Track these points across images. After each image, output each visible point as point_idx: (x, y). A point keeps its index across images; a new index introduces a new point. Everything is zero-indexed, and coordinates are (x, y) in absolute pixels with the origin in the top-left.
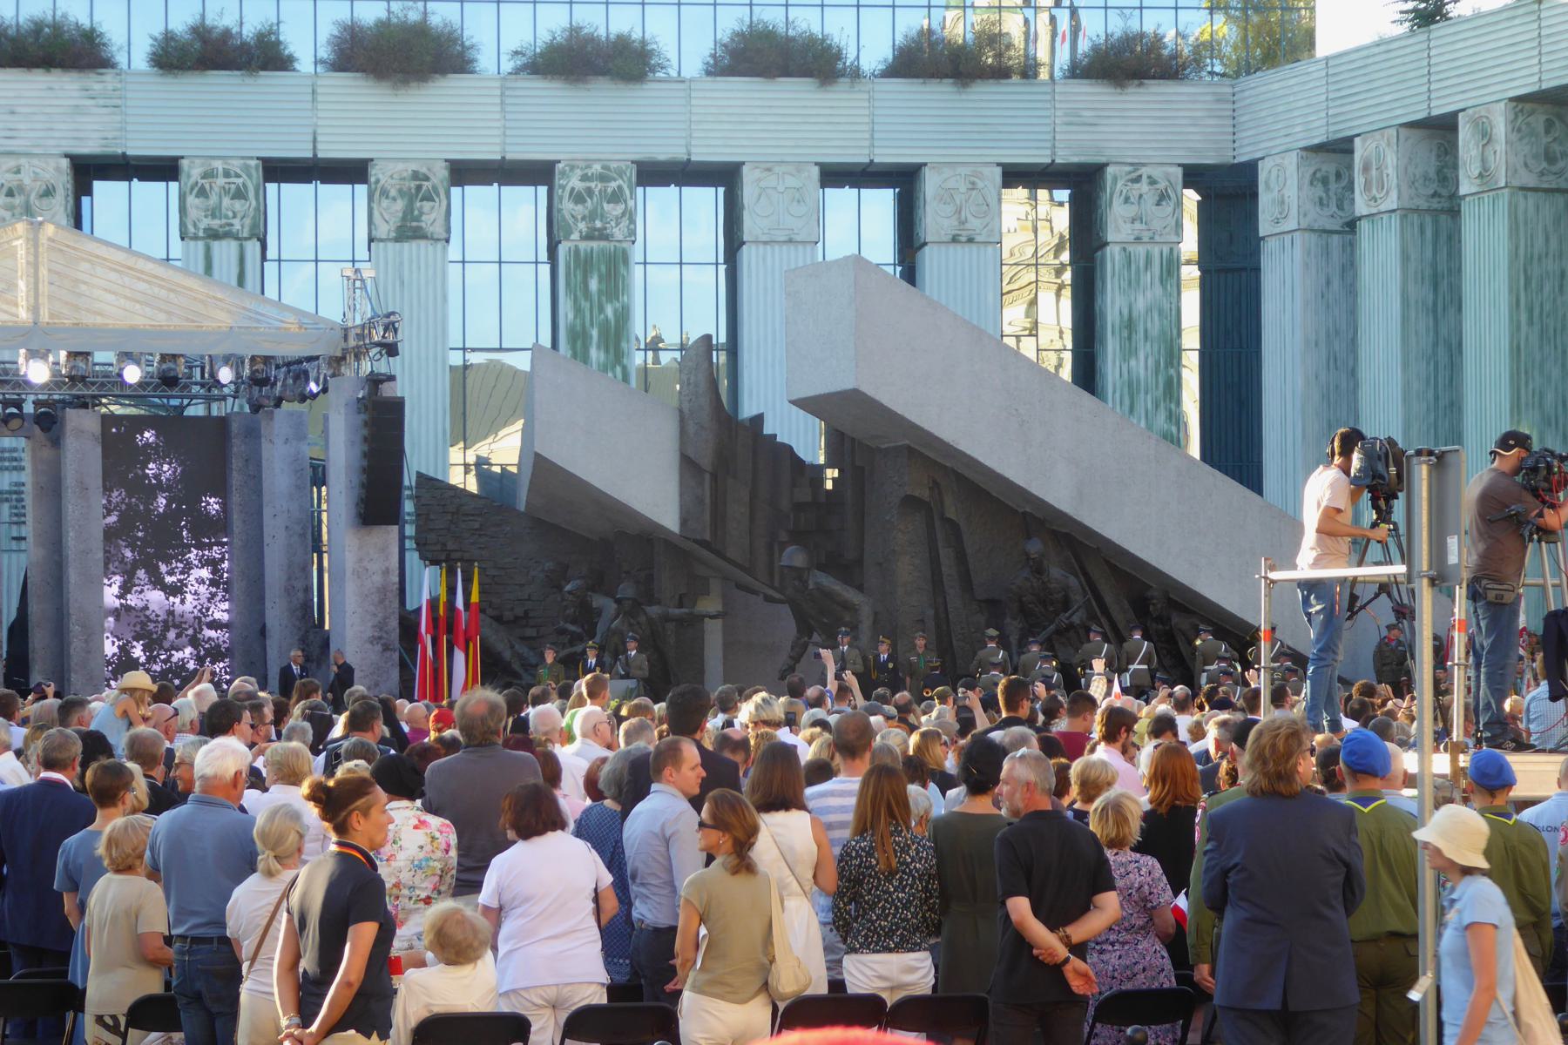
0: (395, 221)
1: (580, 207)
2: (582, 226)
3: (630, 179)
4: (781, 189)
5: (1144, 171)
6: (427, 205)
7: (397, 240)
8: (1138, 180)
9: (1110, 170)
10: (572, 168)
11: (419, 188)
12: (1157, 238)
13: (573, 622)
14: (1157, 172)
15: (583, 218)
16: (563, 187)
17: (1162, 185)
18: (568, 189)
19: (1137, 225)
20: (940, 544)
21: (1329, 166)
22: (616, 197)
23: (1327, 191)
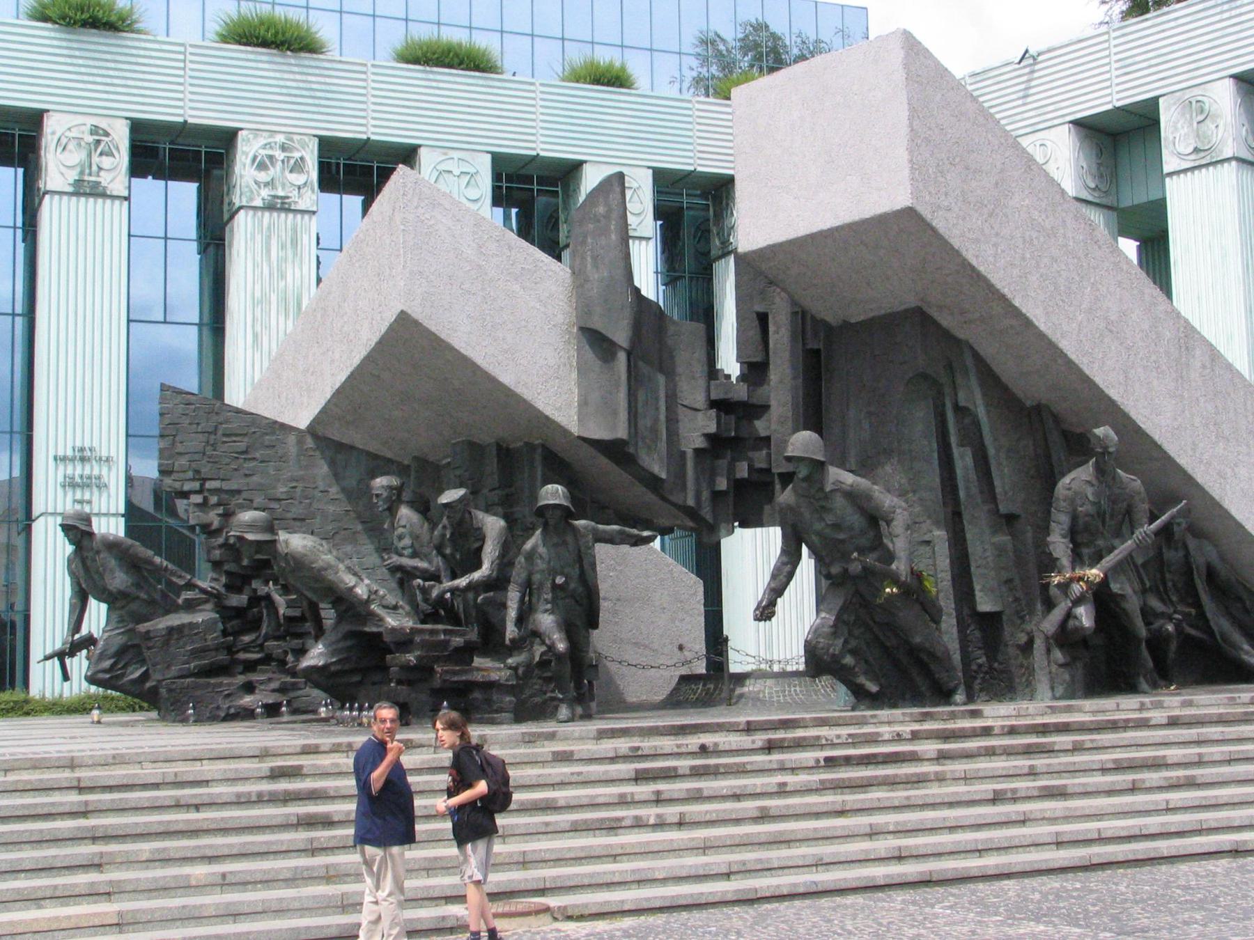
0: (73, 176)
1: (263, 176)
2: (265, 193)
3: (312, 151)
4: (457, 172)
6: (106, 162)
7: (76, 194)
10: (256, 136)
11: (98, 142)
13: (415, 555)
15: (266, 184)
16: (246, 154)
18: (251, 156)
20: (953, 440)
22: (298, 167)
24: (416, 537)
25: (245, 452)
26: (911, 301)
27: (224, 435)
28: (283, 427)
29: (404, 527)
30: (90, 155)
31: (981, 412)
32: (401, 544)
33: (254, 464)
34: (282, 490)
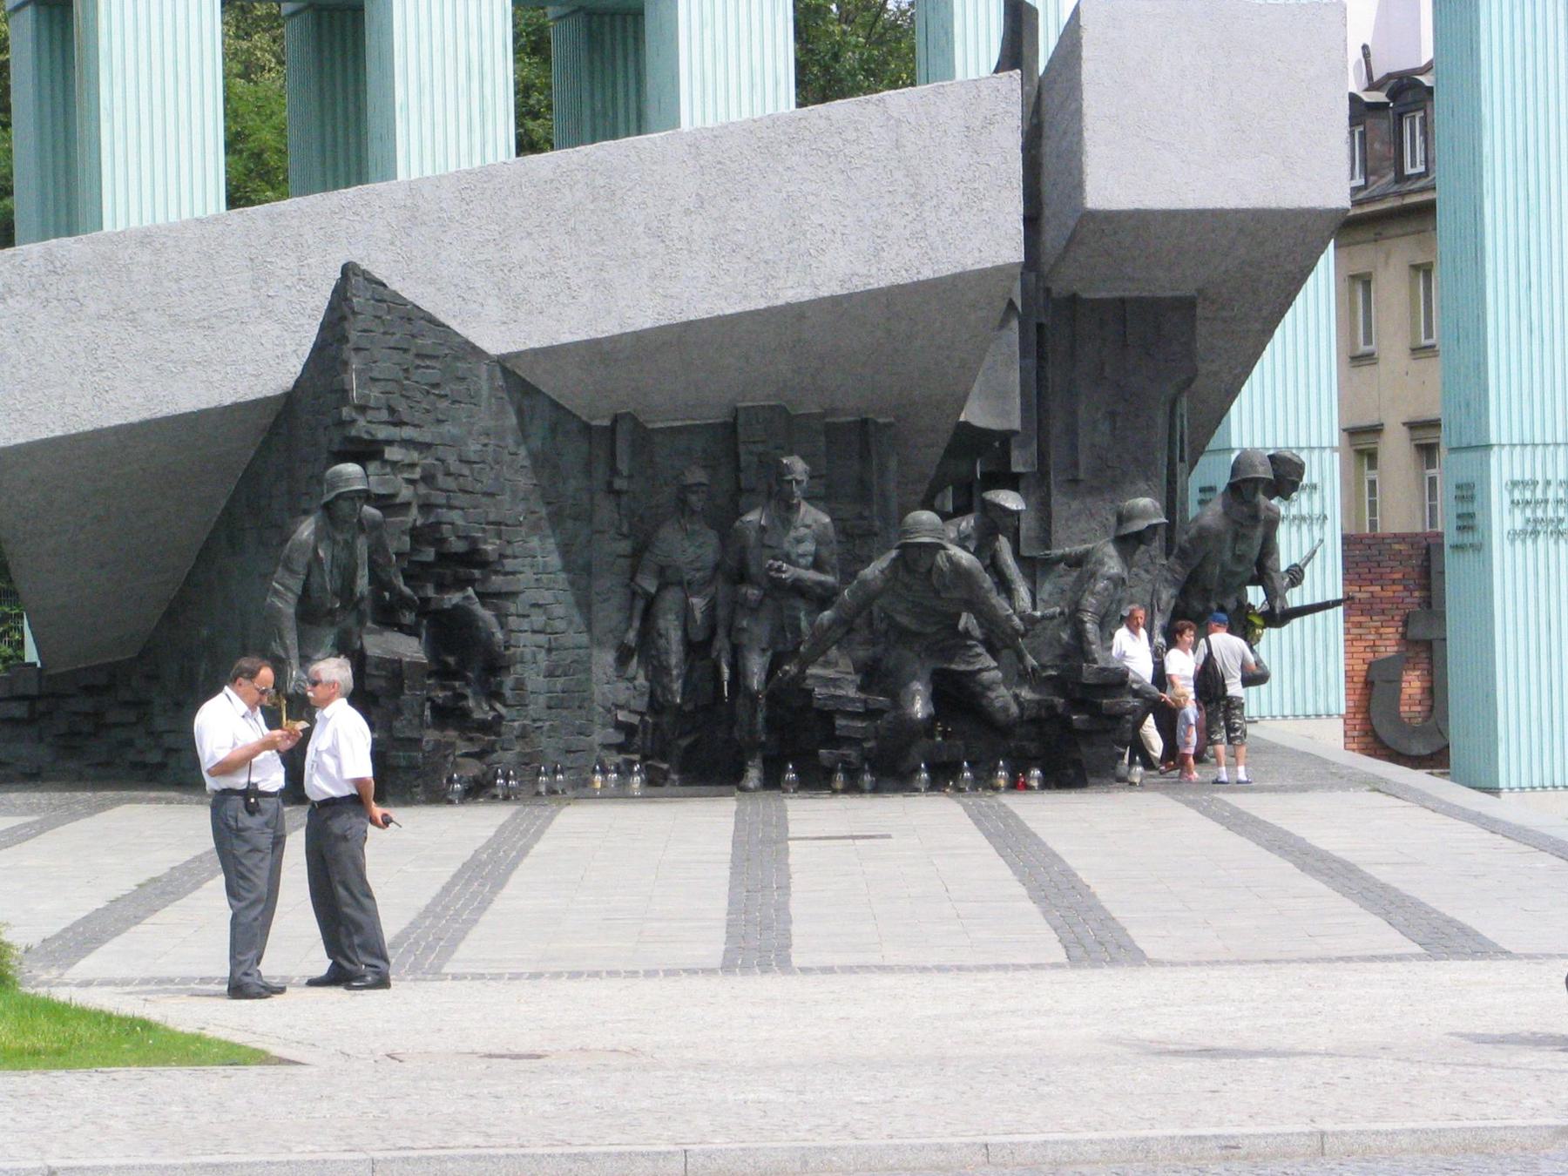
24: (820, 541)
25: (436, 385)
26: (1188, 290)
27: (418, 356)
28: (474, 347)
29: (808, 527)
32: (802, 548)
33: (443, 404)
34: (473, 448)
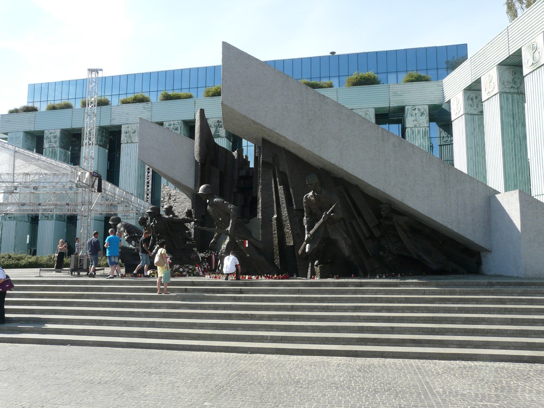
5: (417, 107)
8: (415, 109)
9: (406, 107)
12: (421, 126)
14: (420, 107)
17: (422, 111)
19: (415, 122)
20: (278, 183)
21: (473, 94)
23: (473, 102)
30: (217, 128)
31: (287, 173)
